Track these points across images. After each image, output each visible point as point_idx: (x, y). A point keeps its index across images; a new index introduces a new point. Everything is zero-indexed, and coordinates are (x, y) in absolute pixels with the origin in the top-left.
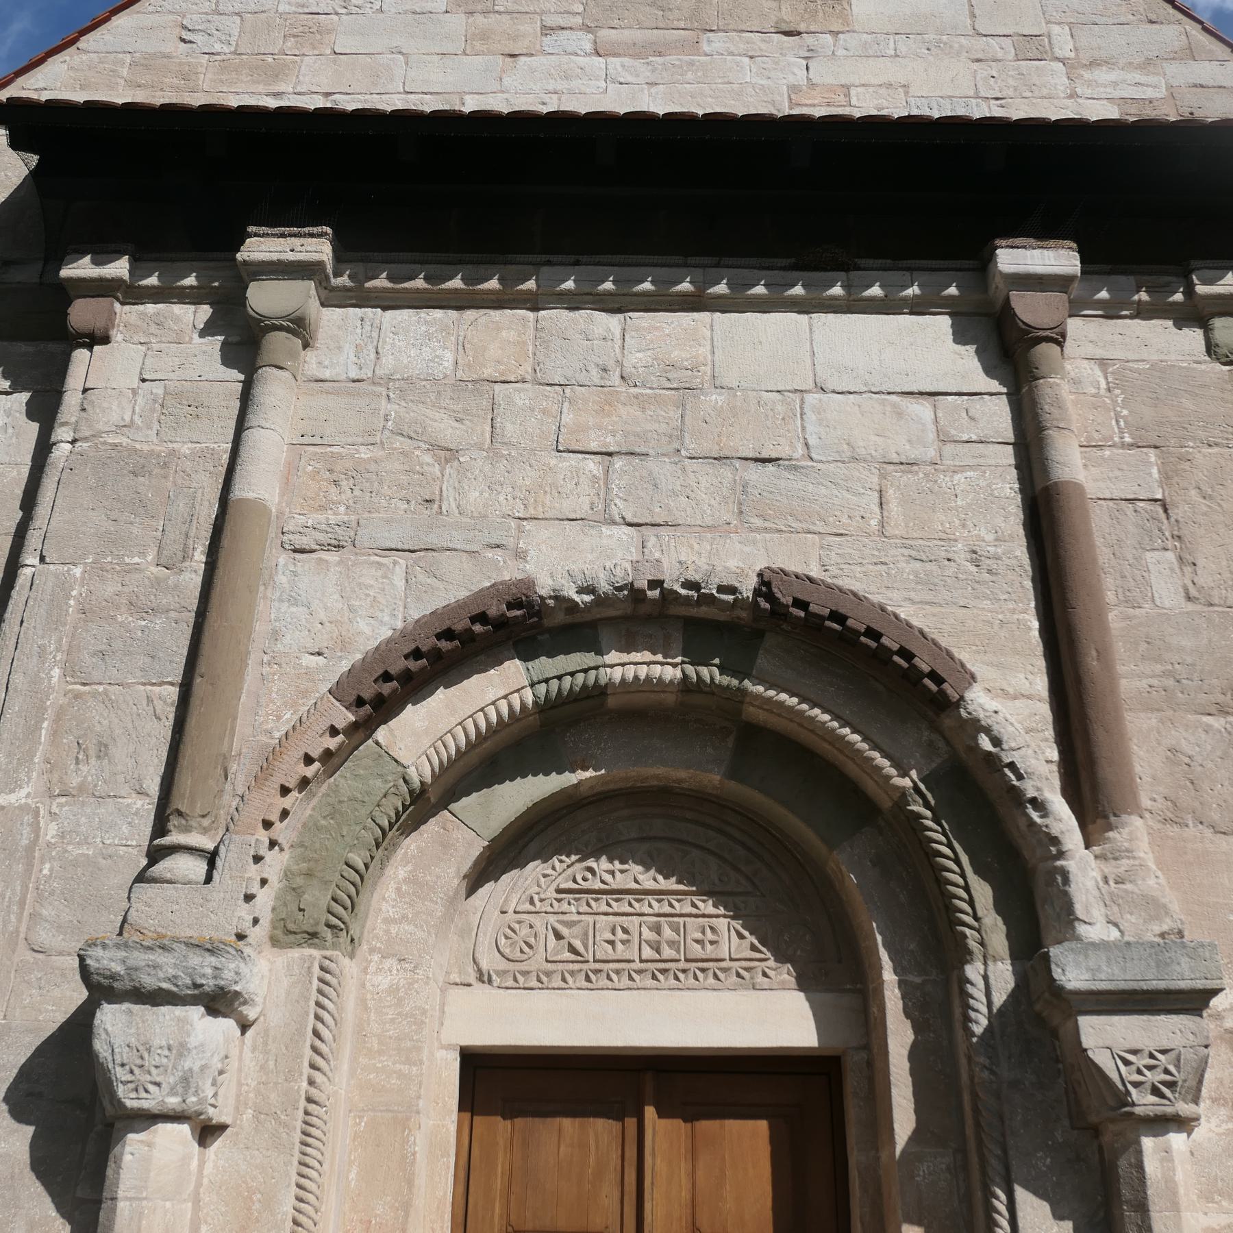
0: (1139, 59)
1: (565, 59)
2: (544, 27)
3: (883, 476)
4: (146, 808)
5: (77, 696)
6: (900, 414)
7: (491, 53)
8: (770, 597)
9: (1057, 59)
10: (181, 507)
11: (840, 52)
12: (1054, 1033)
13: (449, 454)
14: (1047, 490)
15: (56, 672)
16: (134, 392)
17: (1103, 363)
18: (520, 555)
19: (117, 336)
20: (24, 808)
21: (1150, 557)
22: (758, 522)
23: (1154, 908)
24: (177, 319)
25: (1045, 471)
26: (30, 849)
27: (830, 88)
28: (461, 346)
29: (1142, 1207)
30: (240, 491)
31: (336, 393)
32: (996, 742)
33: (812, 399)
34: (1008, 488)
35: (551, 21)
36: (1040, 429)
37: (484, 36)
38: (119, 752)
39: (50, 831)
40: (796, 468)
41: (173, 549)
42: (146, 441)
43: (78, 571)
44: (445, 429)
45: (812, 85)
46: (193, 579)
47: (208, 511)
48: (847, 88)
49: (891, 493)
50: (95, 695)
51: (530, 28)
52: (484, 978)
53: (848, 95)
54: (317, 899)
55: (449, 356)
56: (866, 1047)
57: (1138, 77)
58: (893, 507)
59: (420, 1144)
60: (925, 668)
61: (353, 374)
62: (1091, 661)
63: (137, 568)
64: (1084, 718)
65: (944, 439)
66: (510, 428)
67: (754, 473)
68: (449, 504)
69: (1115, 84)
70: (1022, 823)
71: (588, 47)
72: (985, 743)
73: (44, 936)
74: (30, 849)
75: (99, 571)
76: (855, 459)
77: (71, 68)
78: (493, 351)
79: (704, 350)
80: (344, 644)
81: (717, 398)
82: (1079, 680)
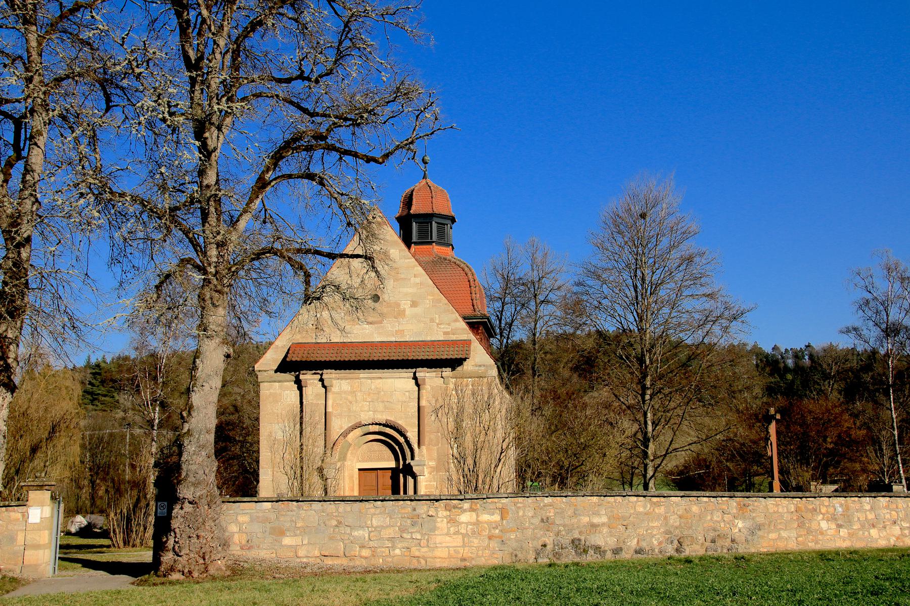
6: (404, 394)
13: (351, 403)
17: (430, 386)
27: (401, 331)
28: (351, 386)
30: (327, 411)
42: (315, 402)
44: (350, 398)
52: (360, 461)
59: (354, 479)
65: (410, 398)
66: (358, 398)
67: (386, 403)
69: (443, 328)
78: (355, 387)
80: (341, 428)
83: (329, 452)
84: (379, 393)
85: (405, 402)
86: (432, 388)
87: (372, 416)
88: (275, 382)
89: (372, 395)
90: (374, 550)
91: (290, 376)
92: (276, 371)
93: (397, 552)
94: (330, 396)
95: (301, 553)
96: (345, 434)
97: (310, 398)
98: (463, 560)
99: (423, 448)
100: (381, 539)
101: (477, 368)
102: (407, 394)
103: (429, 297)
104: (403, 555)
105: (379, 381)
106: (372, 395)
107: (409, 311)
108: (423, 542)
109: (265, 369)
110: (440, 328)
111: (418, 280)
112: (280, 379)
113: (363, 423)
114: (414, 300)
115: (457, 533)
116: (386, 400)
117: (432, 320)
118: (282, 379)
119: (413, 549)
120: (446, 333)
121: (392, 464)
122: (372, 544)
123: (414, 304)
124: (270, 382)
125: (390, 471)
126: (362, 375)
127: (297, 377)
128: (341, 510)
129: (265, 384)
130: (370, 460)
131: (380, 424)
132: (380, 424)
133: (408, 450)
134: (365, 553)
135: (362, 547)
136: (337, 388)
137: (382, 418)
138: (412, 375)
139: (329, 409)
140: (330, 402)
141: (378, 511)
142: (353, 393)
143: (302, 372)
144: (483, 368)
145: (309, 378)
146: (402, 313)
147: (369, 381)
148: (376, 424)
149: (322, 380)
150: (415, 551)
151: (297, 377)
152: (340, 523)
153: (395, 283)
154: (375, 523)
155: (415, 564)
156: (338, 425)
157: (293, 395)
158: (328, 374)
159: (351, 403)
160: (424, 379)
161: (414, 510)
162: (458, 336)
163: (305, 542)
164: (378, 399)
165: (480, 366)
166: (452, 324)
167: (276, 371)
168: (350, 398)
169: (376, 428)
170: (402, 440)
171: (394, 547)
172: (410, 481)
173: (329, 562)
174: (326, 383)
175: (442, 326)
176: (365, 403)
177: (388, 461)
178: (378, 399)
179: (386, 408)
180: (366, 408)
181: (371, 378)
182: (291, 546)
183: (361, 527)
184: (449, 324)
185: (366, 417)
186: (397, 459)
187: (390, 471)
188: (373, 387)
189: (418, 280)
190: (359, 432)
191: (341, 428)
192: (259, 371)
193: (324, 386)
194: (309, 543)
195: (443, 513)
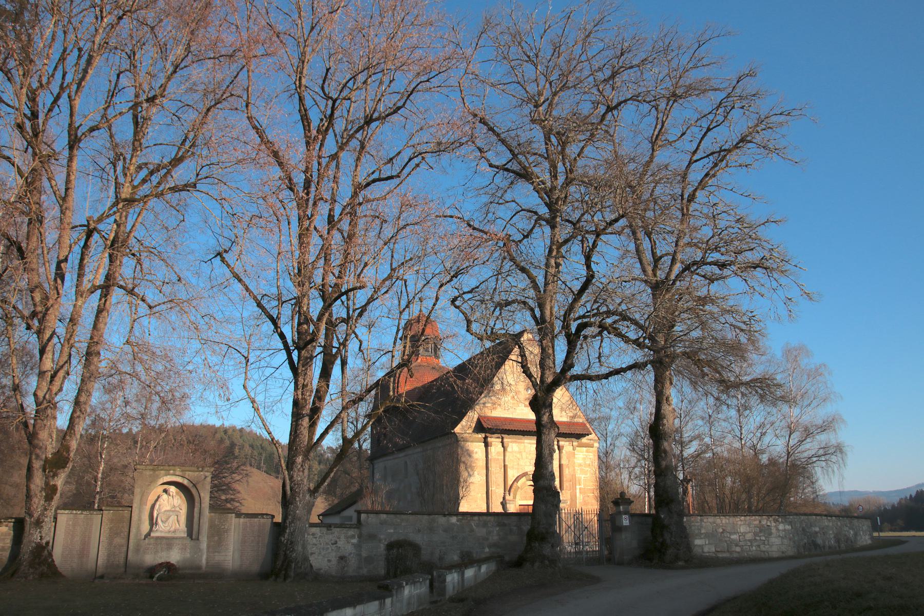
44: (518, 456)
46: (503, 470)
90: (741, 547)
93: (754, 548)
94: (507, 454)
95: (706, 550)
96: (517, 480)
98: (783, 552)
100: (746, 540)
104: (756, 550)
108: (766, 542)
115: (779, 536)
119: (762, 546)
122: (741, 543)
126: (526, 441)
127: (486, 438)
128: (724, 522)
134: (738, 549)
135: (737, 545)
140: (507, 458)
141: (742, 523)
142: (520, 452)
145: (495, 441)
149: (502, 442)
150: (763, 548)
151: (486, 438)
152: (724, 530)
154: (742, 530)
155: (763, 555)
156: (512, 475)
158: (507, 439)
161: (760, 522)
163: (707, 543)
168: (518, 456)
171: (752, 546)
173: (720, 555)
174: (505, 445)
182: (700, 546)
183: (735, 533)
193: (503, 446)
194: (709, 544)
195: (773, 524)
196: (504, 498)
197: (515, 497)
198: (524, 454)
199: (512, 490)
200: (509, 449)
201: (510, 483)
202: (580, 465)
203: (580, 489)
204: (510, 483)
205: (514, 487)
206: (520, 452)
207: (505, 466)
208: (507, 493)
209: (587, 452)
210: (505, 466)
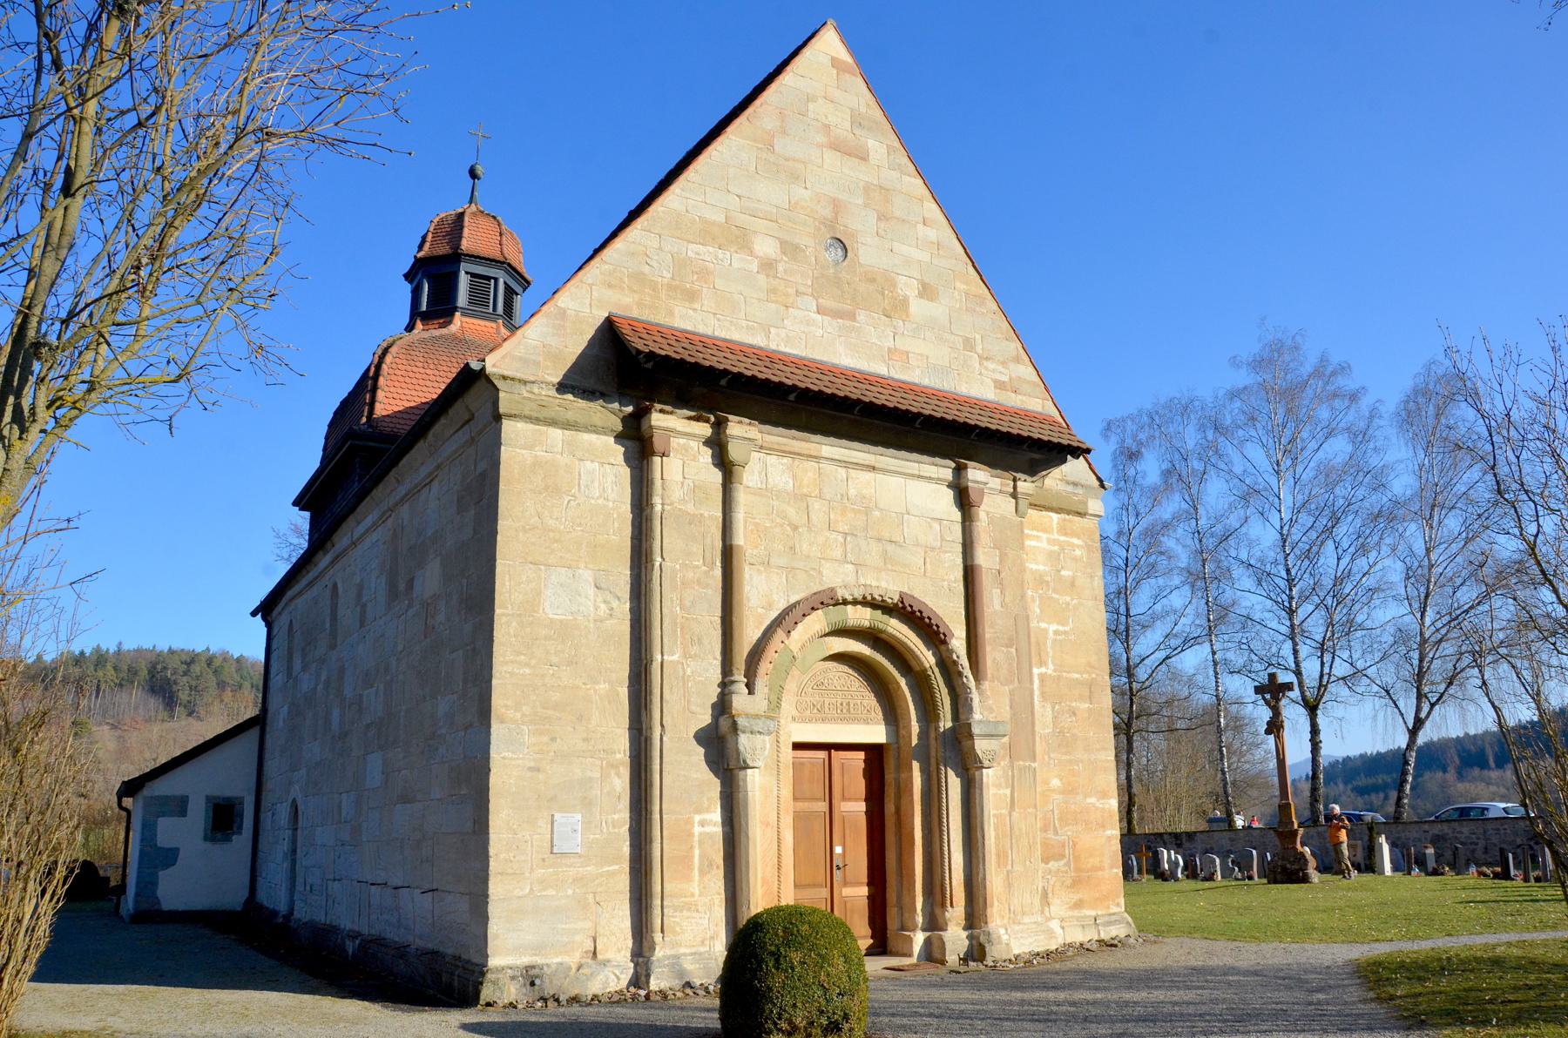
0: (1002, 359)
1: (806, 313)
2: (797, 291)
3: (925, 552)
4: (717, 663)
5: (687, 619)
6: (931, 527)
7: (776, 302)
8: (902, 602)
9: (976, 353)
10: (708, 541)
11: (906, 332)
12: (960, 743)
14: (972, 566)
15: (678, 608)
16: (682, 483)
18: (820, 573)
19: (671, 455)
20: (678, 662)
21: (994, 591)
22: (890, 567)
23: (991, 710)
24: (692, 448)
25: (972, 557)
26: (683, 677)
28: (794, 477)
29: (981, 790)
31: (755, 494)
32: (958, 657)
33: (906, 516)
34: (959, 560)
35: (802, 289)
36: (972, 542)
37: (774, 291)
38: (706, 642)
39: (689, 672)
40: (901, 546)
41: (708, 559)
42: (690, 508)
43: (678, 566)
44: (791, 512)
45: (896, 349)
46: (718, 572)
47: (719, 545)
48: (907, 353)
49: (928, 559)
50: (693, 619)
51: (791, 291)
53: (908, 357)
54: (774, 698)
55: (791, 481)
56: (897, 742)
57: (1001, 368)
58: (928, 565)
60: (942, 631)
61: (759, 486)
62: (980, 630)
63: (697, 567)
64: (976, 647)
65: (942, 539)
66: (814, 517)
68: (797, 550)
69: (993, 371)
70: (960, 683)
71: (815, 308)
72: (955, 657)
73: (693, 708)
74: (683, 677)
75: (684, 565)
76: (918, 545)
77: (601, 273)
78: (805, 482)
79: (873, 491)
81: (877, 513)
82: (976, 636)
83: (739, 677)
84: (867, 511)
85: (933, 549)
86: (992, 521)
87: (851, 579)
88: (552, 423)
89: (850, 515)
91: (609, 414)
92: (562, 387)
94: (741, 497)
96: (784, 620)
97: (676, 493)
99: (986, 685)
101: (1070, 488)
102: (936, 526)
103: (958, 284)
105: (868, 476)
106: (850, 515)
107: (917, 307)
109: (518, 375)
110: (986, 368)
111: (932, 234)
112: (570, 416)
113: (842, 593)
114: (927, 281)
116: (886, 535)
117: (969, 344)
118: (581, 420)
120: (1000, 385)
121: (877, 734)
123: (926, 291)
124: (536, 421)
125: (861, 755)
129: (521, 426)
130: (821, 716)
131: (873, 604)
132: (873, 604)
133: (944, 691)
136: (756, 477)
137: (890, 587)
138: (948, 474)
139: (739, 539)
140: (739, 516)
143: (658, 406)
144: (1080, 491)
146: (898, 308)
147: (842, 472)
148: (865, 603)
153: (882, 225)
157: (610, 478)
159: (795, 528)
160: (982, 493)
162: (1024, 398)
164: (866, 529)
165: (1075, 484)
166: (1012, 366)
167: (562, 387)
169: (861, 617)
170: (928, 658)
172: (954, 784)
175: (991, 366)
176: (834, 535)
177: (866, 722)
178: (866, 529)
179: (885, 556)
180: (838, 553)
181: (846, 464)
184: (1003, 363)
185: (842, 580)
186: (892, 715)
187: (861, 755)
188: (852, 492)
189: (932, 234)
190: (817, 622)
191: (770, 606)
192: (504, 378)
196: (722, 707)
197: (775, 705)
198: (816, 505)
199: (764, 667)
200: (749, 478)
201: (749, 634)
202: (1040, 581)
203: (1042, 677)
204: (749, 634)
205: (770, 654)
206: (801, 498)
207: (728, 554)
208: (739, 677)
209: (1063, 530)
210: (728, 554)
